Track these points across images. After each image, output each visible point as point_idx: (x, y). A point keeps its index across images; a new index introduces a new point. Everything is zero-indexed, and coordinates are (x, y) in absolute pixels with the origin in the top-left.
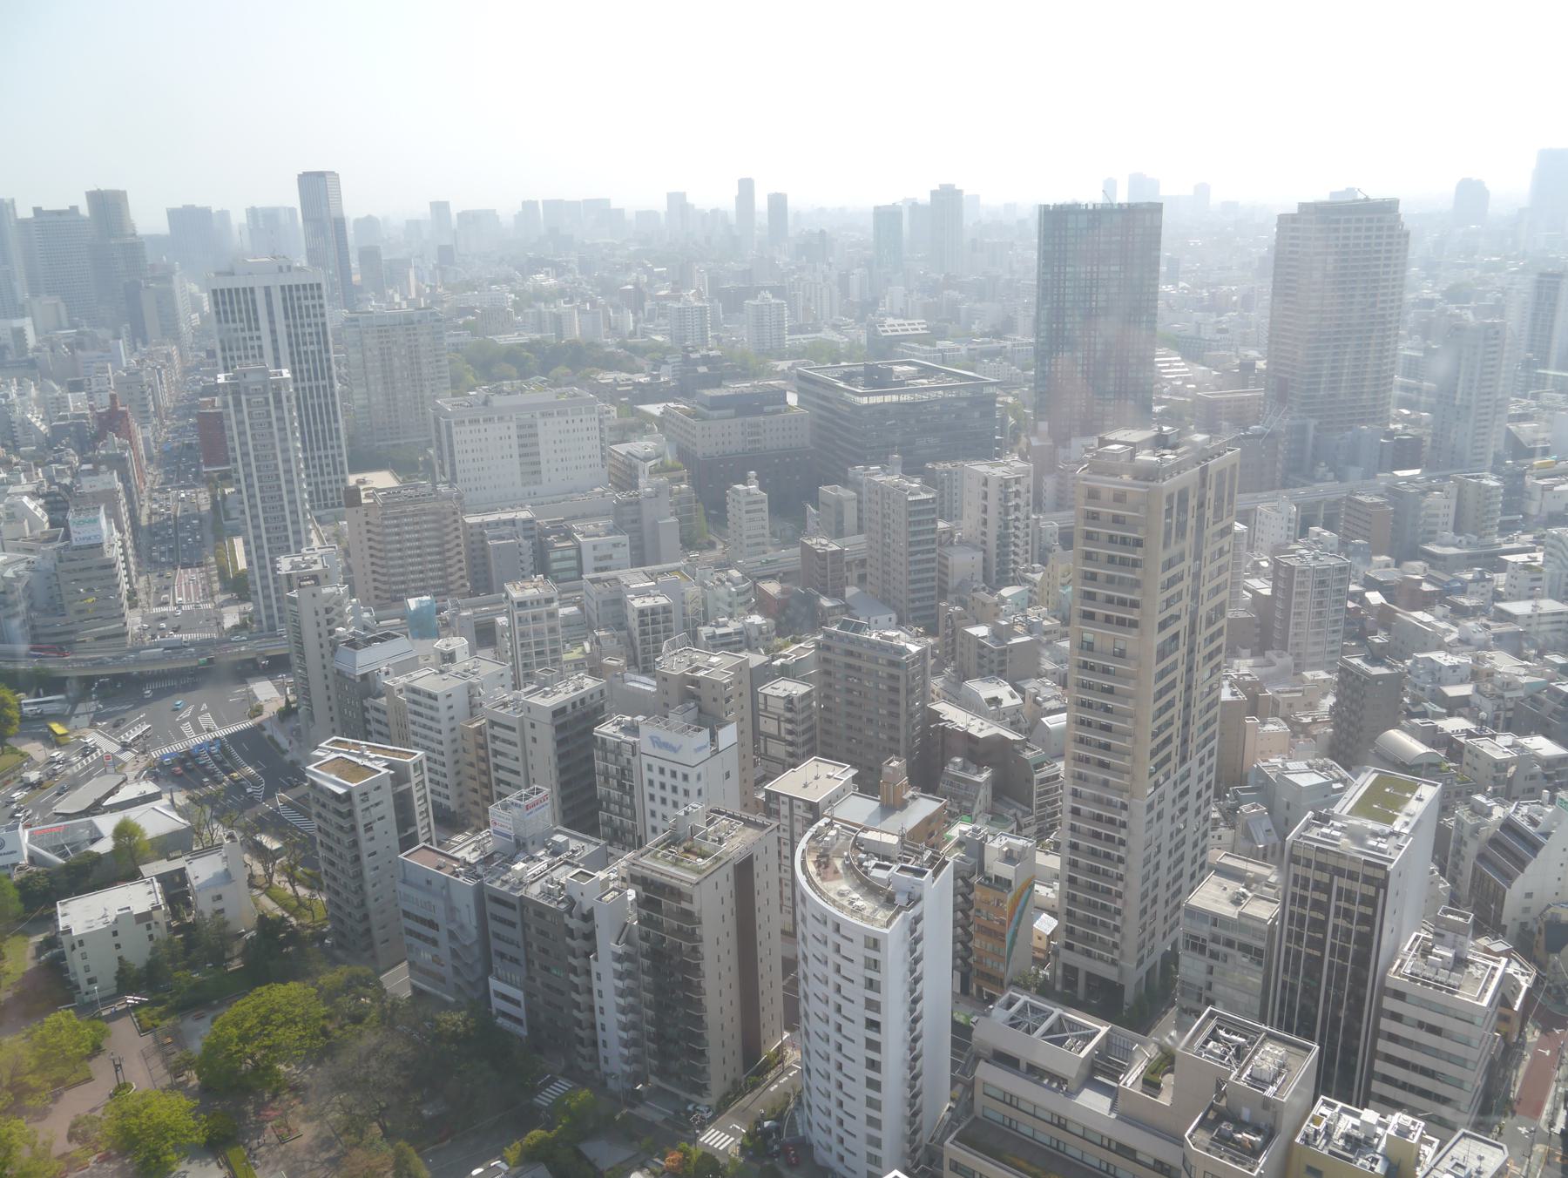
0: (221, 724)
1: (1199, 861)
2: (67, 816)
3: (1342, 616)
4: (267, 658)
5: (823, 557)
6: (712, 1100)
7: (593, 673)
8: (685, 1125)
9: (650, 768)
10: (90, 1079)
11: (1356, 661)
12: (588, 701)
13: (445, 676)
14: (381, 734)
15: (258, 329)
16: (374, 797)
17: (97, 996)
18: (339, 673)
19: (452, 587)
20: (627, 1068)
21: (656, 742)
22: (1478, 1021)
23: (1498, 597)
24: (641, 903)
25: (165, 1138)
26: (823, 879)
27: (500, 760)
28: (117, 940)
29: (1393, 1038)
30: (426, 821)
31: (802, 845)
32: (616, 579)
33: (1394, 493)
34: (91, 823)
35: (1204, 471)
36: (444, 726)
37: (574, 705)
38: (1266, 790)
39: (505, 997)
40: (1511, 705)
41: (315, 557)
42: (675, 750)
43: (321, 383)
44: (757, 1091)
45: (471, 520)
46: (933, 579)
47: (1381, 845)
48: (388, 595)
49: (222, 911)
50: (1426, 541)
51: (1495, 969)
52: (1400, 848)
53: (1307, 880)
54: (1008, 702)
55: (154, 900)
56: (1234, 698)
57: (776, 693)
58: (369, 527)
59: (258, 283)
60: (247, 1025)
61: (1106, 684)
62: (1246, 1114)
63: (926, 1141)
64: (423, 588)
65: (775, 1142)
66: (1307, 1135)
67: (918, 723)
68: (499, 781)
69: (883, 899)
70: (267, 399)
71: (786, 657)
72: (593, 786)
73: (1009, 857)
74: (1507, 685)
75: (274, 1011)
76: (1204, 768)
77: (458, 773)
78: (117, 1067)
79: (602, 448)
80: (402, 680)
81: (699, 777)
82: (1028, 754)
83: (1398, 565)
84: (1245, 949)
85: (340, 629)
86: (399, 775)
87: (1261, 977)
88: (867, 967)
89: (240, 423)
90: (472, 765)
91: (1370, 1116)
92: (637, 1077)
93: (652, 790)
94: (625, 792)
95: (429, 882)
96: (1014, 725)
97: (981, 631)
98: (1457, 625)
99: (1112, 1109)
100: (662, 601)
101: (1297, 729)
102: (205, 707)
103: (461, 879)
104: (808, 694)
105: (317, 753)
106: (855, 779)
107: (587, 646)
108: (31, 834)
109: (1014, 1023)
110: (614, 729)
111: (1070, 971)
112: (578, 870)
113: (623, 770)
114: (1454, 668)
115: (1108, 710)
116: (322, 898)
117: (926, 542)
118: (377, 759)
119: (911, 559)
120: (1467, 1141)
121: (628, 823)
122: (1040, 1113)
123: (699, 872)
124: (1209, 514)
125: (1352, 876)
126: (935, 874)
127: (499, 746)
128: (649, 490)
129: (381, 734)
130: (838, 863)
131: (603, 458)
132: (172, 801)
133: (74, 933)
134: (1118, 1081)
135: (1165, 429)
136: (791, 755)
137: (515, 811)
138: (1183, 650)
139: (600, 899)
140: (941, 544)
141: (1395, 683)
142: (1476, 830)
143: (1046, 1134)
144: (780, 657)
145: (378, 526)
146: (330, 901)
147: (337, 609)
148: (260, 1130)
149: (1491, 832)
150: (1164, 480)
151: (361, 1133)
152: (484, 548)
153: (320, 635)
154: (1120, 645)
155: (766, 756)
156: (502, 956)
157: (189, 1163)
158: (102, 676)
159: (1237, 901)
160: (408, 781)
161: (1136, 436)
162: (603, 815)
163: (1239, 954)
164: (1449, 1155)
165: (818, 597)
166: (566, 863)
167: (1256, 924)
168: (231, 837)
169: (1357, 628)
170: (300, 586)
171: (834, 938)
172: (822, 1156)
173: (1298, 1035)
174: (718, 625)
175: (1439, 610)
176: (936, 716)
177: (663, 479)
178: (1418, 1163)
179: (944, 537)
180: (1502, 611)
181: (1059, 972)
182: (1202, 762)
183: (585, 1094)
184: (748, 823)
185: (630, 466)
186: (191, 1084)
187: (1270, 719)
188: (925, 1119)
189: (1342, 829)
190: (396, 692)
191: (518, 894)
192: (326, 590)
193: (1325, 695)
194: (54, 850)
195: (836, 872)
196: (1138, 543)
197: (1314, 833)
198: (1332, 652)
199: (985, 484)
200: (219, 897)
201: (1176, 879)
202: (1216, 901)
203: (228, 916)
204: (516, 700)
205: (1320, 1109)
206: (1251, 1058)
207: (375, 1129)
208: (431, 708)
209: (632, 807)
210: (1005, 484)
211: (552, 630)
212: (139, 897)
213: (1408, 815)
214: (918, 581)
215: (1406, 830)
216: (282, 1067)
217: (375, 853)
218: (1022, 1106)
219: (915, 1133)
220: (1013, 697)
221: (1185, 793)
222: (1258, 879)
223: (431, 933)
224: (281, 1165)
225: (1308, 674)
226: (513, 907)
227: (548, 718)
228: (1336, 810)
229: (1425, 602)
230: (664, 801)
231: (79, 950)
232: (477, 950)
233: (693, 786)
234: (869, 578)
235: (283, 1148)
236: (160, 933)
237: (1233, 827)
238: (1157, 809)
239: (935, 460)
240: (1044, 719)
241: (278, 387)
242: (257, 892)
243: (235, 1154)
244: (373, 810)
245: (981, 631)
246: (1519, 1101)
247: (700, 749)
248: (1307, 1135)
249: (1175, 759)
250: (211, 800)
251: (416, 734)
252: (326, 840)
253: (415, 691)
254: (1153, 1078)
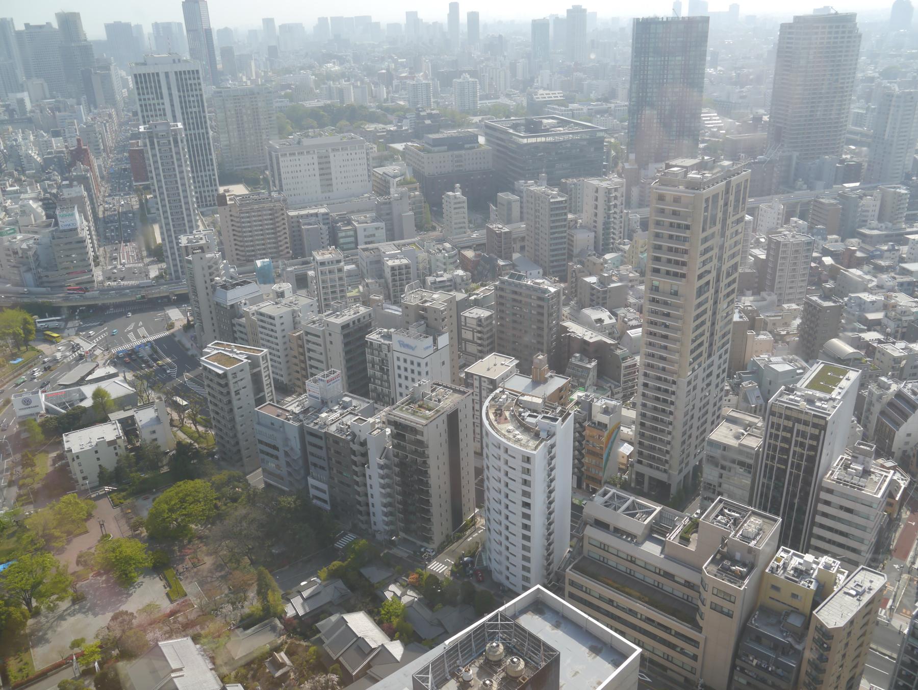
0: (151, 334)
1: (717, 414)
2: (66, 386)
3: (807, 271)
4: (176, 295)
5: (500, 235)
6: (435, 545)
7: (365, 304)
8: (420, 559)
9: (398, 359)
10: (87, 532)
11: (815, 298)
12: (362, 320)
13: (279, 306)
14: (243, 339)
15: (162, 98)
16: (240, 375)
17: (88, 486)
18: (218, 304)
19: (281, 253)
20: (387, 528)
21: (402, 344)
22: (875, 506)
23: (902, 260)
24: (394, 436)
25: (130, 564)
26: (498, 423)
27: (312, 354)
28: (97, 455)
29: (825, 515)
30: (270, 389)
31: (486, 403)
32: (377, 249)
33: (843, 197)
34: (80, 390)
35: (728, 183)
36: (279, 334)
37: (354, 322)
38: (758, 373)
39: (317, 488)
40: (905, 324)
41: (201, 236)
42: (413, 348)
43: (201, 131)
44: (460, 541)
45: (292, 213)
46: (564, 249)
47: (823, 406)
48: (244, 258)
49: (156, 440)
50: (860, 227)
51: (886, 477)
52: (835, 407)
53: (779, 425)
54: (607, 321)
55: (117, 433)
56: (741, 320)
57: (471, 316)
58: (232, 218)
59: (161, 70)
60: (173, 503)
61: (666, 311)
62: (738, 556)
63: (556, 569)
64: (264, 254)
65: (471, 569)
66: (772, 568)
67: (554, 334)
68: (312, 367)
69: (533, 434)
70: (169, 141)
71: (477, 294)
72: (365, 369)
73: (606, 411)
74: (904, 313)
75: (187, 495)
76: (722, 360)
77: (288, 362)
78: (102, 525)
79: (369, 170)
80: (254, 308)
81: (427, 364)
82: (618, 352)
83: (843, 241)
84: (742, 464)
85: (217, 278)
86: (254, 362)
87: (750, 480)
88: (523, 472)
89: (154, 156)
90: (295, 357)
91: (809, 558)
92: (392, 533)
94: (384, 373)
95: (272, 424)
96: (611, 335)
97: (592, 280)
98: (876, 277)
99: (662, 553)
100: (405, 261)
101: (778, 338)
102: (141, 323)
103: (291, 422)
104: (490, 317)
105: (206, 350)
106: (517, 366)
107: (361, 288)
108: (46, 396)
109: (607, 504)
110: (377, 336)
111: (640, 476)
112: (357, 417)
113: (383, 361)
114: (873, 303)
115: (666, 326)
116: (212, 432)
117: (561, 226)
118: (241, 353)
119: (552, 236)
120: (864, 572)
121: (386, 391)
122: (621, 554)
123: (427, 419)
124: (731, 209)
125: (806, 423)
126: (563, 420)
127: (311, 346)
128: (396, 195)
129: (243, 339)
130: (507, 414)
131: (369, 176)
132: (125, 377)
133: (73, 452)
134: (665, 537)
135: (706, 158)
136: (480, 352)
137: (321, 384)
138: (712, 291)
139: (370, 434)
140: (569, 228)
141: (838, 311)
142: (880, 397)
143: (623, 566)
144: (474, 294)
145: (237, 217)
146: (216, 434)
147: (215, 267)
148: (182, 560)
149: (889, 398)
150: (704, 189)
151: (238, 562)
152: (300, 231)
154: (675, 288)
155: (466, 352)
156: (315, 465)
157: (144, 577)
158: (81, 306)
159: (738, 437)
160: (259, 366)
161: (689, 162)
162: (371, 386)
163: (738, 467)
164: (853, 580)
165: (496, 260)
166: (351, 413)
167: (749, 450)
168: (159, 398)
169: (816, 278)
170: (193, 253)
171: (504, 456)
172: (496, 577)
173: (770, 512)
174: (437, 276)
175: (866, 268)
176: (565, 329)
177: (405, 189)
178: (835, 584)
179: (572, 224)
180: (904, 269)
181: (634, 476)
182: (720, 357)
183: (363, 542)
184: (455, 391)
185: (385, 181)
186: (143, 535)
187: (762, 332)
188: (555, 557)
189: (801, 396)
190: (251, 315)
191: (323, 431)
192: (209, 256)
193: (795, 318)
194: (59, 405)
195: (506, 419)
196: (687, 227)
197: (785, 398)
198: (800, 293)
199: (597, 191)
200: (154, 432)
201: (703, 424)
202: (726, 437)
203: (159, 442)
204: (321, 319)
205: (780, 553)
206: (742, 525)
207: (246, 560)
208: (271, 324)
209: (388, 381)
210: (608, 191)
211: (341, 279)
212: (109, 432)
213: (840, 388)
214: (556, 250)
215: (839, 397)
216: (193, 526)
217: (241, 407)
218: (611, 550)
219: (549, 564)
220: (610, 318)
221: (710, 374)
222: (750, 425)
223: (274, 452)
224: (195, 579)
225: (785, 306)
226: (321, 438)
227: (339, 330)
228: (798, 385)
229: (858, 263)
230: (406, 378)
231: (77, 461)
233: (423, 369)
234: (527, 248)
235: (195, 570)
236: (122, 452)
237: (737, 394)
238: (693, 384)
239: (567, 177)
240: (628, 332)
241: (176, 132)
242: (175, 429)
243: (170, 573)
244: (239, 383)
245: (592, 280)
246: (895, 550)
247: (427, 348)
248: (772, 568)
249: (705, 355)
250: (147, 377)
251: (263, 339)
252: (213, 400)
253: (261, 314)
254: (685, 536)
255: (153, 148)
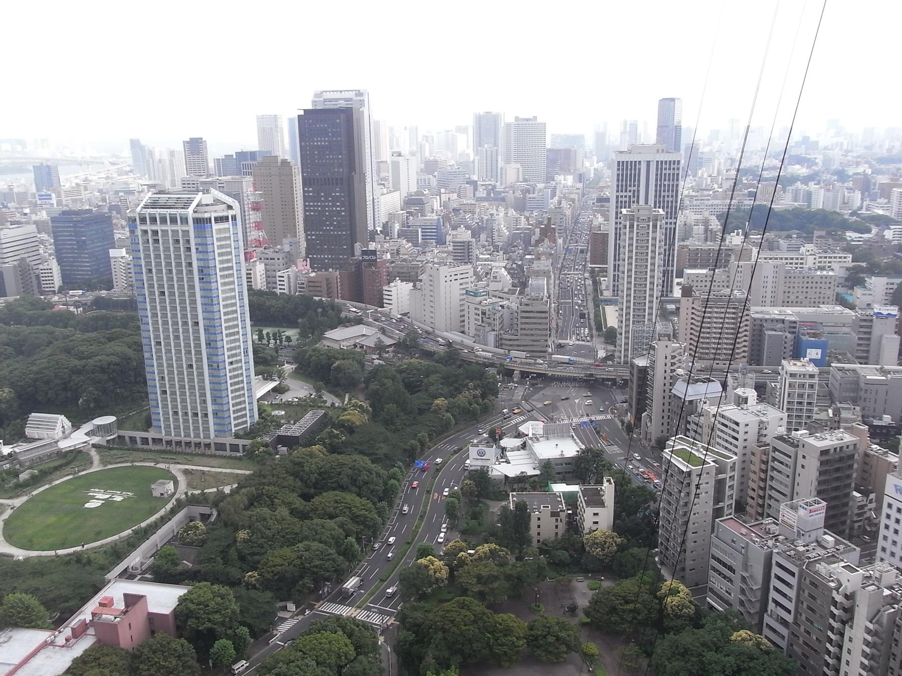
9: (890, 506)
12: (845, 448)
36: (740, 443)
59: (643, 158)
93: (888, 522)
107: (830, 411)
153: (665, 372)
158: (534, 373)
232: (759, 594)
255: (631, 232)
